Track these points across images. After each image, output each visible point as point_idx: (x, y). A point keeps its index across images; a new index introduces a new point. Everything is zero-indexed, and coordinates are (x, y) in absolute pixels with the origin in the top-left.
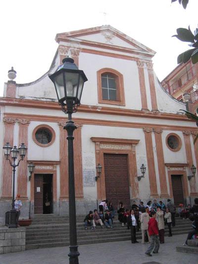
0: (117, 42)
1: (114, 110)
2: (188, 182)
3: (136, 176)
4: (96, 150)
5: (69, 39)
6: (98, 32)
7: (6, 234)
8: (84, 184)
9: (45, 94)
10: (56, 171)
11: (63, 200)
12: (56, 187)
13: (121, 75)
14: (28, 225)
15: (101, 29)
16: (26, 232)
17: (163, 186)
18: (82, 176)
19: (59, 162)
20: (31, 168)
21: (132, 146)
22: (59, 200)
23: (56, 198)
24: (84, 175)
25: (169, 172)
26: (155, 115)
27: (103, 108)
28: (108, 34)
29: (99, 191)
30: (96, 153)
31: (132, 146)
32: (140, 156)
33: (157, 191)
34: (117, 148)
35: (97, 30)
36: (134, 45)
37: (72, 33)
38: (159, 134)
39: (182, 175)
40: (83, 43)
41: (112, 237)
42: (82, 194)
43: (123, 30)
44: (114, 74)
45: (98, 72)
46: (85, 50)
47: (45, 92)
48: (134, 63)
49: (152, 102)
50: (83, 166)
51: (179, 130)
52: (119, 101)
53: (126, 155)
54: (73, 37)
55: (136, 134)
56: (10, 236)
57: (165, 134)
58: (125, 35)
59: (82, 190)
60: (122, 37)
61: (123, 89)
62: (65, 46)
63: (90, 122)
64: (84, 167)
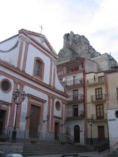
0: (45, 45)
1: (44, 84)
2: (61, 127)
3: (43, 120)
4: (28, 101)
5: (27, 34)
6: (39, 36)
7: (15, 146)
8: (21, 120)
9: (10, 61)
10: (9, 109)
11: (10, 128)
12: (7, 119)
13: (44, 64)
14: (35, 143)
15: (41, 36)
16: (24, 146)
17: (52, 127)
18: (20, 115)
19: (11, 104)
20: (31, 113)
21: (43, 103)
22: (8, 127)
23: (6, 126)
24: (21, 114)
25: (54, 120)
26: (54, 90)
27: (36, 79)
28: (42, 40)
29: (27, 124)
30: (28, 103)
31: (43, 103)
32: (46, 108)
33: (49, 130)
34: (37, 103)
35: (39, 35)
36: (51, 50)
37: (29, 31)
38: (53, 99)
39: (59, 123)
40: (32, 39)
41: (53, 152)
42: (19, 125)
43: (50, 41)
44: (40, 61)
45: (35, 58)
46: (32, 44)
47: (10, 60)
48: (49, 59)
49: (53, 83)
50: (22, 109)
51: (60, 100)
52: (41, 77)
53: (40, 107)
54: (29, 34)
55: (44, 97)
56: (16, 147)
57: (56, 100)
58: (49, 44)
59: (19, 123)
60: (48, 44)
61: (44, 71)
62: (24, 37)
63: (11, 77)
64: (22, 110)
